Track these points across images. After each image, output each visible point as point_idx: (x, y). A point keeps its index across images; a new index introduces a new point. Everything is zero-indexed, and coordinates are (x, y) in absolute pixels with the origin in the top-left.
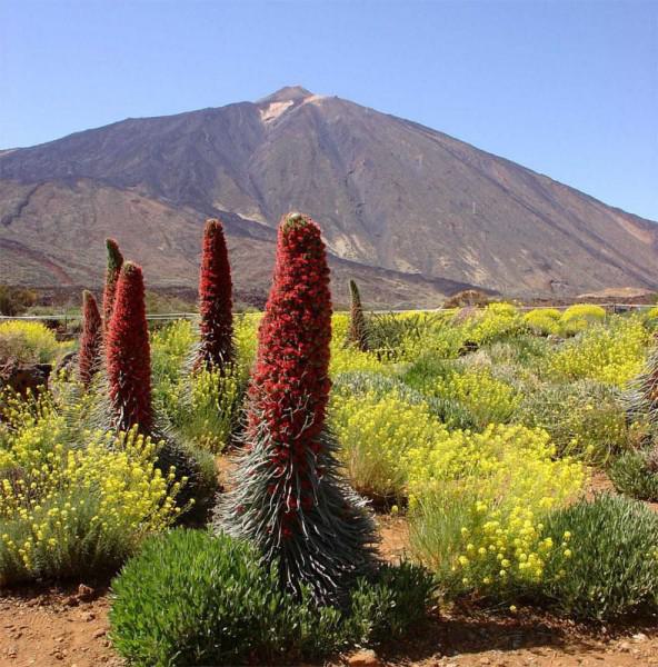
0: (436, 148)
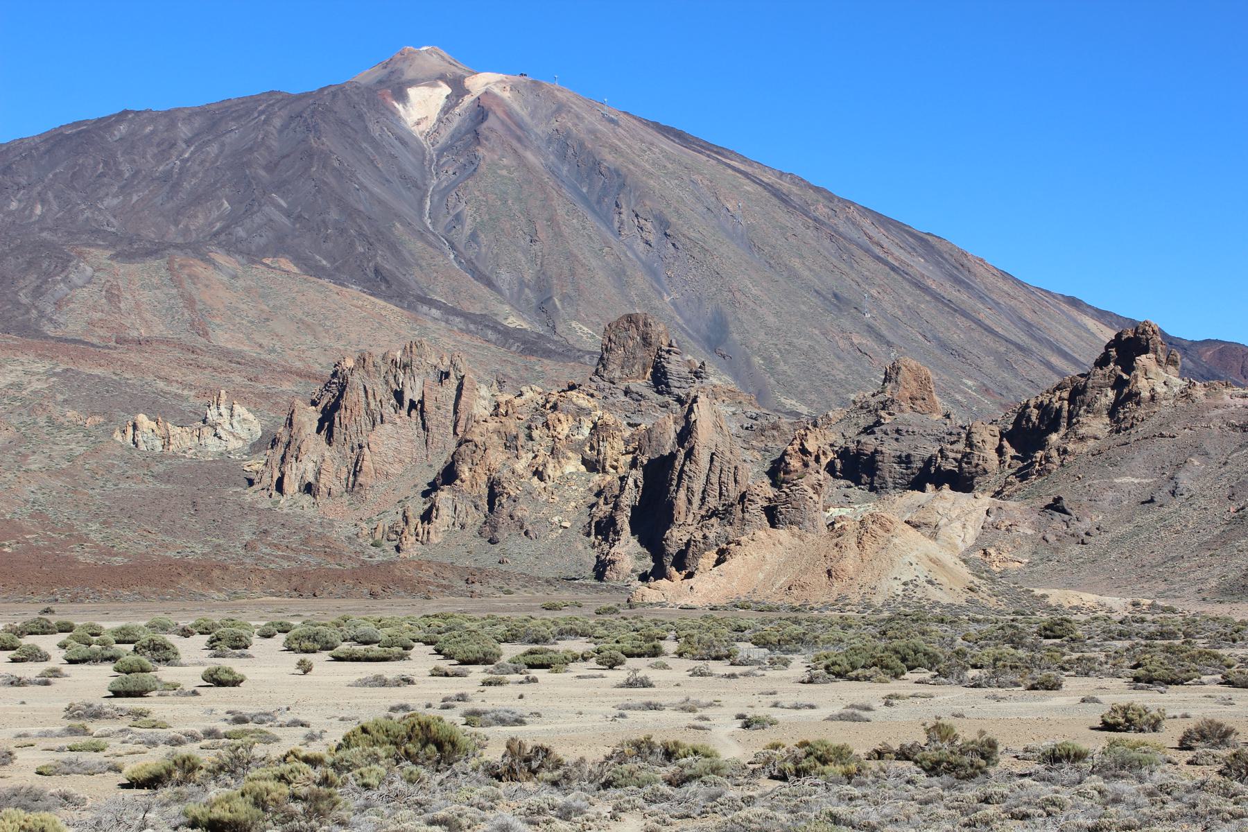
0: (749, 187)
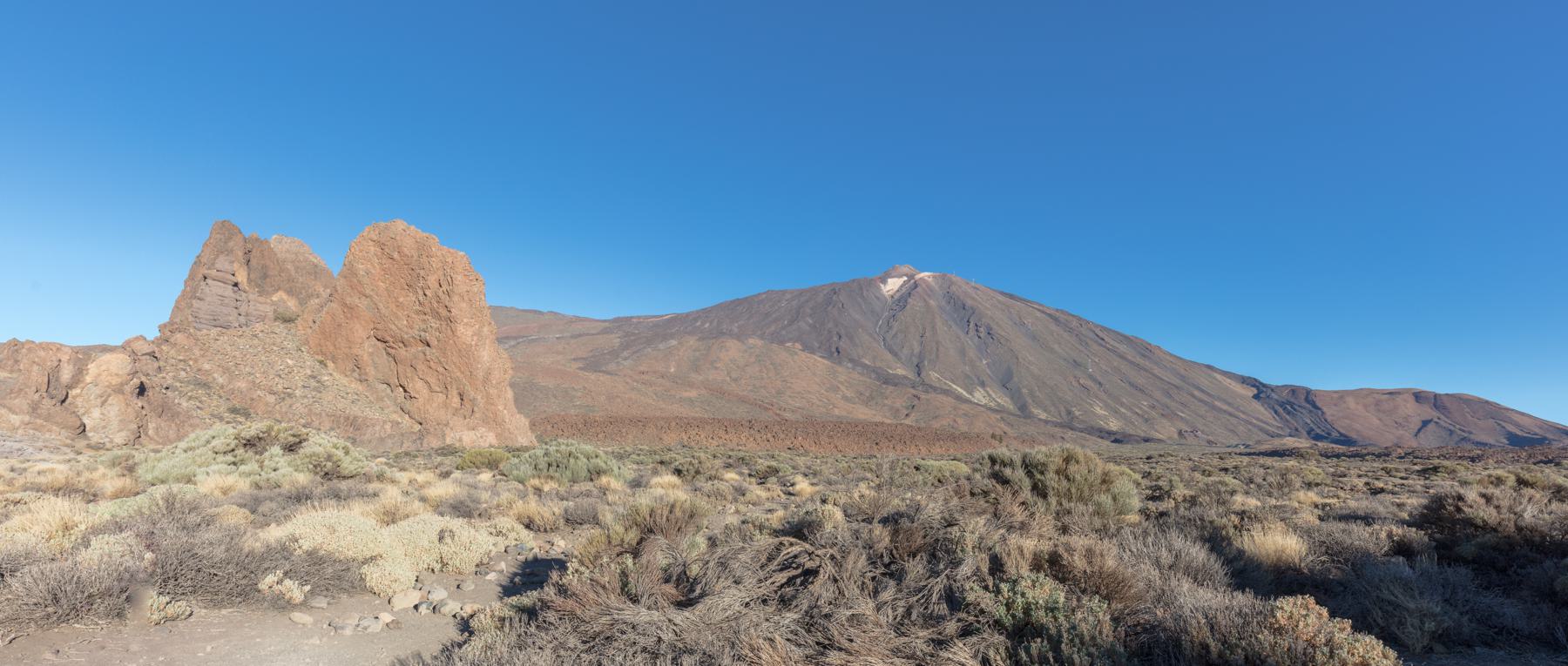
0: (1038, 314)
